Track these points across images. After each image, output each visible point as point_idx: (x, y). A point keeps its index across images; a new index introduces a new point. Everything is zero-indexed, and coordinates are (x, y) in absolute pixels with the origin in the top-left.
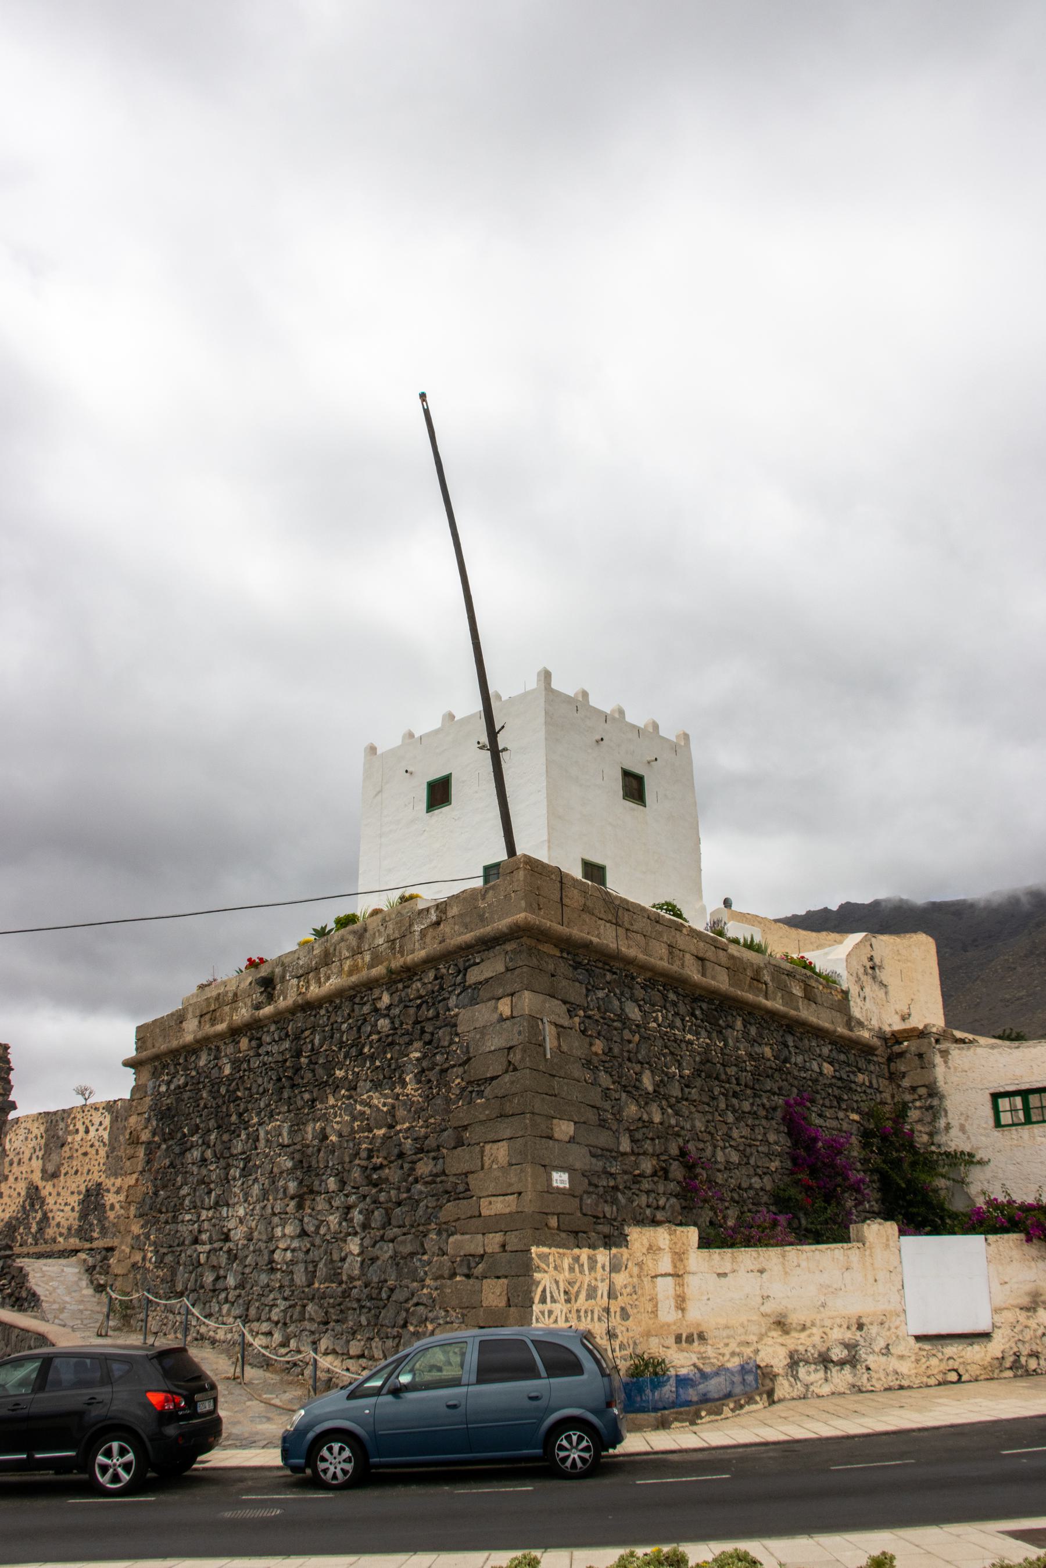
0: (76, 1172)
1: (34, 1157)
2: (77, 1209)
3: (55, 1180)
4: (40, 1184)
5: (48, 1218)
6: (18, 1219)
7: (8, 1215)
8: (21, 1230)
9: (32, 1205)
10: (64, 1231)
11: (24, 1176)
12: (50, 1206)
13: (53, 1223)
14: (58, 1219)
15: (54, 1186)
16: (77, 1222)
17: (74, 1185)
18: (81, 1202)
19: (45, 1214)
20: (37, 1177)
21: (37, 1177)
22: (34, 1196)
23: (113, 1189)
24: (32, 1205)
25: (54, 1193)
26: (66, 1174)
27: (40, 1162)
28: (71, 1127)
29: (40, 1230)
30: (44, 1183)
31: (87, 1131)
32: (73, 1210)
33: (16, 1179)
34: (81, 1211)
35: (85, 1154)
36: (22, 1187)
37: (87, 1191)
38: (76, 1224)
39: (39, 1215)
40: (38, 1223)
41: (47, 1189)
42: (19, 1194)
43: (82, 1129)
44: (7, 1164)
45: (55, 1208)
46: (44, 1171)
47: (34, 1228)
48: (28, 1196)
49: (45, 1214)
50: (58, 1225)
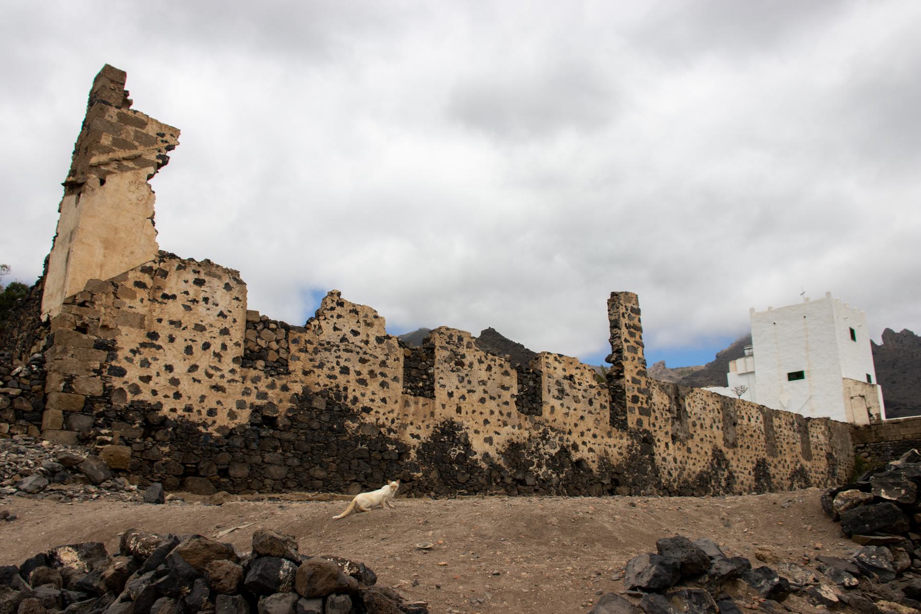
0: (748, 447)
1: (714, 426)
2: (752, 473)
3: (735, 450)
4: (724, 449)
5: (734, 477)
6: (708, 473)
7: (699, 469)
8: (713, 483)
10: (747, 488)
11: (709, 439)
12: (734, 468)
13: (739, 481)
14: (741, 479)
15: (734, 453)
16: (754, 483)
17: (748, 456)
18: (754, 469)
19: (731, 473)
20: (720, 443)
21: (720, 443)
22: (718, 457)
23: (773, 465)
24: (719, 464)
25: (735, 459)
26: (741, 446)
27: (721, 432)
28: (738, 413)
29: (728, 484)
31: (749, 420)
32: (750, 473)
33: (702, 440)
34: (755, 475)
36: (708, 448)
38: (754, 484)
39: (726, 473)
40: (725, 480)
41: (729, 454)
42: (706, 453)
43: (746, 417)
44: (690, 425)
45: (738, 470)
46: (726, 440)
47: (723, 484)
48: (714, 454)
49: (731, 473)
50: (742, 483)
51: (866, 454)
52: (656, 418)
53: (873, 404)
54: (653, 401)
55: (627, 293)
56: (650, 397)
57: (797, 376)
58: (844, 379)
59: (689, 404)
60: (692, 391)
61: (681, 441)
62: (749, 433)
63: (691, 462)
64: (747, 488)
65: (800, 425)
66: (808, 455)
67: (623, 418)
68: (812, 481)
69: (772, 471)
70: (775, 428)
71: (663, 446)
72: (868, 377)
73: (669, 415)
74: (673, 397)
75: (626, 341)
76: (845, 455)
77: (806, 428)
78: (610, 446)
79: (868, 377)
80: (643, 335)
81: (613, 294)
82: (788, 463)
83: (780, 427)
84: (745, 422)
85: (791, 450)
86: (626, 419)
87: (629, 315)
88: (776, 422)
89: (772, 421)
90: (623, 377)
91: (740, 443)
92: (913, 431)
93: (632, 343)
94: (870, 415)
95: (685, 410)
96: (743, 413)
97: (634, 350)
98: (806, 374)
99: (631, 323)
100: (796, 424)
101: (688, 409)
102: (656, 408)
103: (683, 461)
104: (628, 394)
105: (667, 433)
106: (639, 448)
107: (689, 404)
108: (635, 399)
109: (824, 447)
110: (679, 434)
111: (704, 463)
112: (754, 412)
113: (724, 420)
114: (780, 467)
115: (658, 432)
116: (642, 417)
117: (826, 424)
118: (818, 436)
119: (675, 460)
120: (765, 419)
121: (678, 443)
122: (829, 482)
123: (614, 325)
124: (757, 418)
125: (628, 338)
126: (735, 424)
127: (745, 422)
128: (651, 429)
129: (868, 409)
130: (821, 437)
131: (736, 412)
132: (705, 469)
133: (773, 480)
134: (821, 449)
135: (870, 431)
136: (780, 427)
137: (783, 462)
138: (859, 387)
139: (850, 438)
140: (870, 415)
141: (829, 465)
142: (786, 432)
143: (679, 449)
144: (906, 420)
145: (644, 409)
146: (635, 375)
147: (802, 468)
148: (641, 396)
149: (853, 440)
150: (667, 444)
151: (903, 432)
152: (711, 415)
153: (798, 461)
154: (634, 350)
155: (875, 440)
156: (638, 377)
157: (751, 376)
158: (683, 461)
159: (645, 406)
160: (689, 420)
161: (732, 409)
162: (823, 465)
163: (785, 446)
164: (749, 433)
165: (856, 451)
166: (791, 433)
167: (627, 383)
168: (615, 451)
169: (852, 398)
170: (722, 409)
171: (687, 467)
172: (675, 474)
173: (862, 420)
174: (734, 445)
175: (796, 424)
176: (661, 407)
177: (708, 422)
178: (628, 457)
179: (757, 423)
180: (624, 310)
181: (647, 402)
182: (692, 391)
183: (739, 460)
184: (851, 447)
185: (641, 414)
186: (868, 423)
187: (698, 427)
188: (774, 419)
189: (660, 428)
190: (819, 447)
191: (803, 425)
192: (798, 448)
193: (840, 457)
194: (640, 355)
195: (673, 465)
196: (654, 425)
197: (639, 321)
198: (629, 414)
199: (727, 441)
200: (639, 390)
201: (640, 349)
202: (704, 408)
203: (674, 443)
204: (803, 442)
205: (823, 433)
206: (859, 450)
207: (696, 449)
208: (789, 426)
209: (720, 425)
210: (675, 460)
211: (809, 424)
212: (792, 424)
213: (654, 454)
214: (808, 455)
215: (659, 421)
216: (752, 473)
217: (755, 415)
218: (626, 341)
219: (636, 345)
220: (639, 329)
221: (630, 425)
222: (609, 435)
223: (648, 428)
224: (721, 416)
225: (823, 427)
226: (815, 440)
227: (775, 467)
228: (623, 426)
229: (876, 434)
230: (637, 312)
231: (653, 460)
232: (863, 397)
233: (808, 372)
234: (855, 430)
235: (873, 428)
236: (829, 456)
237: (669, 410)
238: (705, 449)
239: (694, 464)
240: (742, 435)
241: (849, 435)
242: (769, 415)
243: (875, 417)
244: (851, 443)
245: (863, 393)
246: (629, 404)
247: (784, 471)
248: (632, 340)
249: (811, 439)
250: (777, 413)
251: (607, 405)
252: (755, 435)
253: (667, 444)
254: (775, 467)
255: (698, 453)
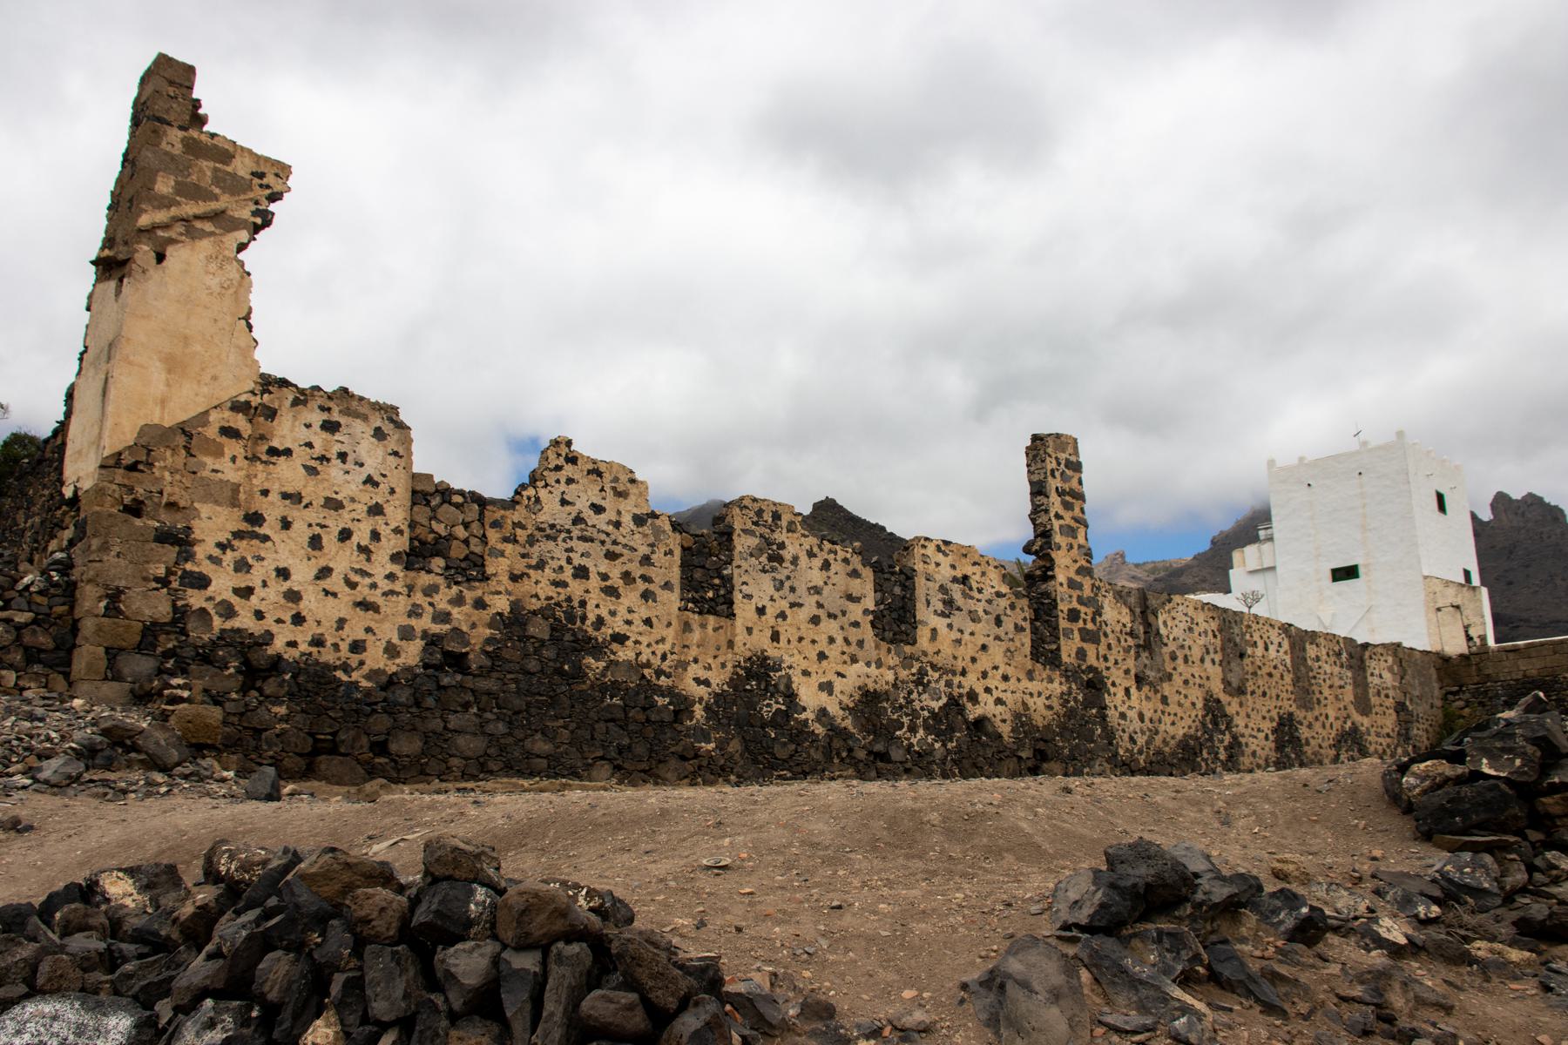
0: (1264, 694)
1: (1208, 659)
2: (1271, 737)
3: (1243, 698)
4: (1224, 698)
5: (1240, 744)
6: (1197, 739)
7: (1181, 732)
8: (1205, 755)
9: (1215, 724)
10: (1262, 762)
11: (1198, 680)
12: (1241, 729)
13: (1248, 751)
14: (1253, 747)
15: (1241, 705)
17: (1265, 709)
18: (1274, 731)
19: (1235, 737)
20: (1217, 687)
21: (1217, 687)
22: (1214, 709)
23: (1305, 723)
24: (1215, 724)
25: (1243, 714)
26: (1253, 693)
27: (1218, 669)
29: (1230, 757)
30: (1228, 699)
31: (1267, 649)
32: (1267, 738)
33: (1186, 682)
34: (1276, 741)
35: (1270, 675)
36: (1196, 695)
37: (1280, 718)
39: (1227, 738)
40: (1225, 749)
42: (1193, 704)
43: (1260, 644)
44: (1167, 658)
45: (1247, 732)
46: (1226, 683)
47: (1223, 756)
49: (1235, 737)
50: (1254, 754)
51: (1461, 703)
52: (1109, 647)
53: (1473, 619)
54: (1104, 617)
55: (1058, 436)
56: (1098, 612)
57: (1347, 573)
58: (1426, 577)
59: (1165, 623)
60: (1170, 601)
61: (1151, 684)
62: (1265, 670)
63: (1167, 719)
64: (1262, 762)
65: (1351, 656)
66: (1364, 707)
67: (1054, 647)
68: (1372, 749)
69: (1304, 733)
70: (1309, 662)
71: (1121, 694)
72: (1467, 574)
73: (1131, 642)
74: (1138, 610)
75: (1058, 516)
76: (1426, 711)
77: (1362, 660)
78: (1031, 694)
79: (1467, 574)
80: (1086, 507)
81: (1035, 438)
82: (1331, 719)
83: (1318, 659)
84: (1259, 651)
85: (1337, 697)
86: (1058, 649)
87: (1062, 474)
88: (1311, 651)
89: (1304, 650)
90: (1053, 577)
91: (1250, 687)
92: (1539, 664)
93: (1068, 520)
94: (1469, 638)
95: (1158, 633)
96: (1256, 637)
97: (1070, 532)
98: (1361, 571)
99: (1066, 487)
100: (1344, 655)
101: (1163, 631)
102: (1108, 630)
103: (1155, 718)
104: (1061, 606)
105: (1127, 672)
106: (1080, 698)
107: (1165, 623)
108: (1074, 615)
109: (1391, 693)
110: (1148, 672)
111: (1189, 722)
112: (1274, 636)
113: (1223, 649)
114: (1317, 726)
115: (1113, 670)
116: (1085, 645)
117: (1395, 655)
118: (1382, 674)
119: (1141, 717)
120: (1292, 646)
121: (1146, 689)
122: (1400, 750)
123: (1038, 490)
124: (1280, 645)
125: (1061, 512)
126: (1242, 656)
127: (1259, 651)
128: (1101, 665)
129: (1466, 628)
130: (1387, 675)
131: (1243, 635)
132: (1192, 731)
133: (1306, 748)
134: (1387, 696)
135: (1470, 665)
136: (1318, 659)
137: (1322, 718)
138: (1451, 591)
139: (1435, 676)
140: (1469, 638)
141: (1400, 722)
142: (1327, 668)
143: (1148, 698)
144: (1529, 646)
145: (1088, 631)
146: (1072, 575)
147: (1355, 729)
148: (1083, 609)
149: (1440, 679)
150: (1127, 691)
151: (1523, 665)
152: (1202, 641)
153: (1349, 716)
154: (1070, 532)
155: (1476, 679)
156: (1078, 579)
157: (1269, 575)
158: (1155, 718)
159: (1090, 626)
160: (1165, 650)
161: (1236, 630)
162: (1389, 722)
163: (1326, 692)
164: (1265, 670)
165: (1444, 698)
166: (1337, 669)
167: (1059, 589)
168: (1040, 702)
169: (1439, 610)
170: (1220, 631)
171: (1162, 728)
172: (1141, 740)
173: (1455, 646)
174: (1241, 691)
175: (1344, 655)
176: (1118, 628)
177: (1196, 653)
178: (1062, 712)
179: (1279, 654)
180: (1054, 465)
181: (1093, 620)
182: (1170, 601)
183: (1248, 716)
184: (1437, 693)
185: (1083, 640)
186: (1465, 651)
187: (1180, 661)
188: (1308, 646)
189: (1116, 663)
190: (1383, 693)
191: (1356, 655)
192: (1349, 694)
193: (1418, 709)
194: (1081, 540)
195: (1137, 725)
196: (1106, 659)
197: (1080, 483)
198: (1062, 641)
199: (1229, 684)
200: (1080, 600)
201: (1082, 531)
202: (1190, 629)
203: (1139, 689)
204: (1356, 684)
205: (1390, 669)
206: (1451, 697)
207: (1176, 698)
208: (1333, 658)
209: (1218, 658)
210: (1141, 717)
211: (1367, 654)
212: (1339, 654)
213: (1105, 708)
214: (1364, 707)
215: (1114, 651)
216: (1271, 737)
217: (1276, 641)
218: (1058, 516)
219: (1073, 524)
220: (1080, 497)
221: (1065, 658)
222: (1030, 675)
223: (1095, 664)
224: (1218, 642)
225: (1390, 659)
226: (1376, 680)
227: (1310, 726)
228: (1053, 660)
229: (1479, 670)
230: (1077, 467)
231: (1104, 717)
232: (1458, 607)
233: (1366, 566)
234: (1443, 663)
235: (1474, 660)
236: (1400, 707)
237: (1131, 634)
238: (1192, 698)
239: (1173, 724)
240: (1255, 674)
241: (1433, 671)
242: (1299, 640)
243: (1478, 641)
244: (1436, 685)
245: (1458, 601)
246: (1063, 624)
247: (1324, 733)
248: (1067, 515)
249: (1370, 679)
250: (1313, 636)
251: (1027, 625)
252: (1276, 674)
253: (1127, 691)
254: (1310, 726)
255: (1180, 705)
